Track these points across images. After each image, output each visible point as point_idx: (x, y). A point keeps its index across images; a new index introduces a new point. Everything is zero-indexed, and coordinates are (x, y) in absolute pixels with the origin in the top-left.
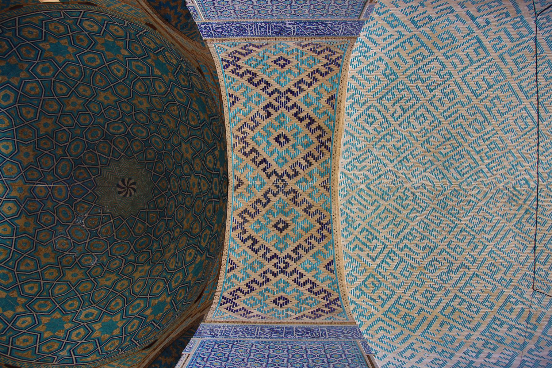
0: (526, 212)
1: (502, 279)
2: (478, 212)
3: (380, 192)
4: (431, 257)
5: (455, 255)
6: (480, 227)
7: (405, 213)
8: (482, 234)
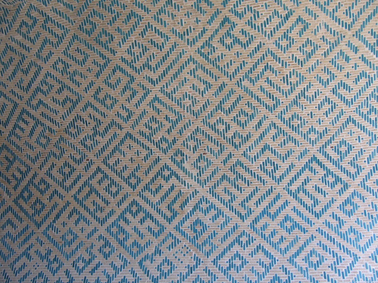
0: (223, 24)
1: (164, 139)
2: (142, 34)
4: (74, 114)
5: (102, 108)
6: (143, 60)
7: (35, 49)
8: (146, 72)
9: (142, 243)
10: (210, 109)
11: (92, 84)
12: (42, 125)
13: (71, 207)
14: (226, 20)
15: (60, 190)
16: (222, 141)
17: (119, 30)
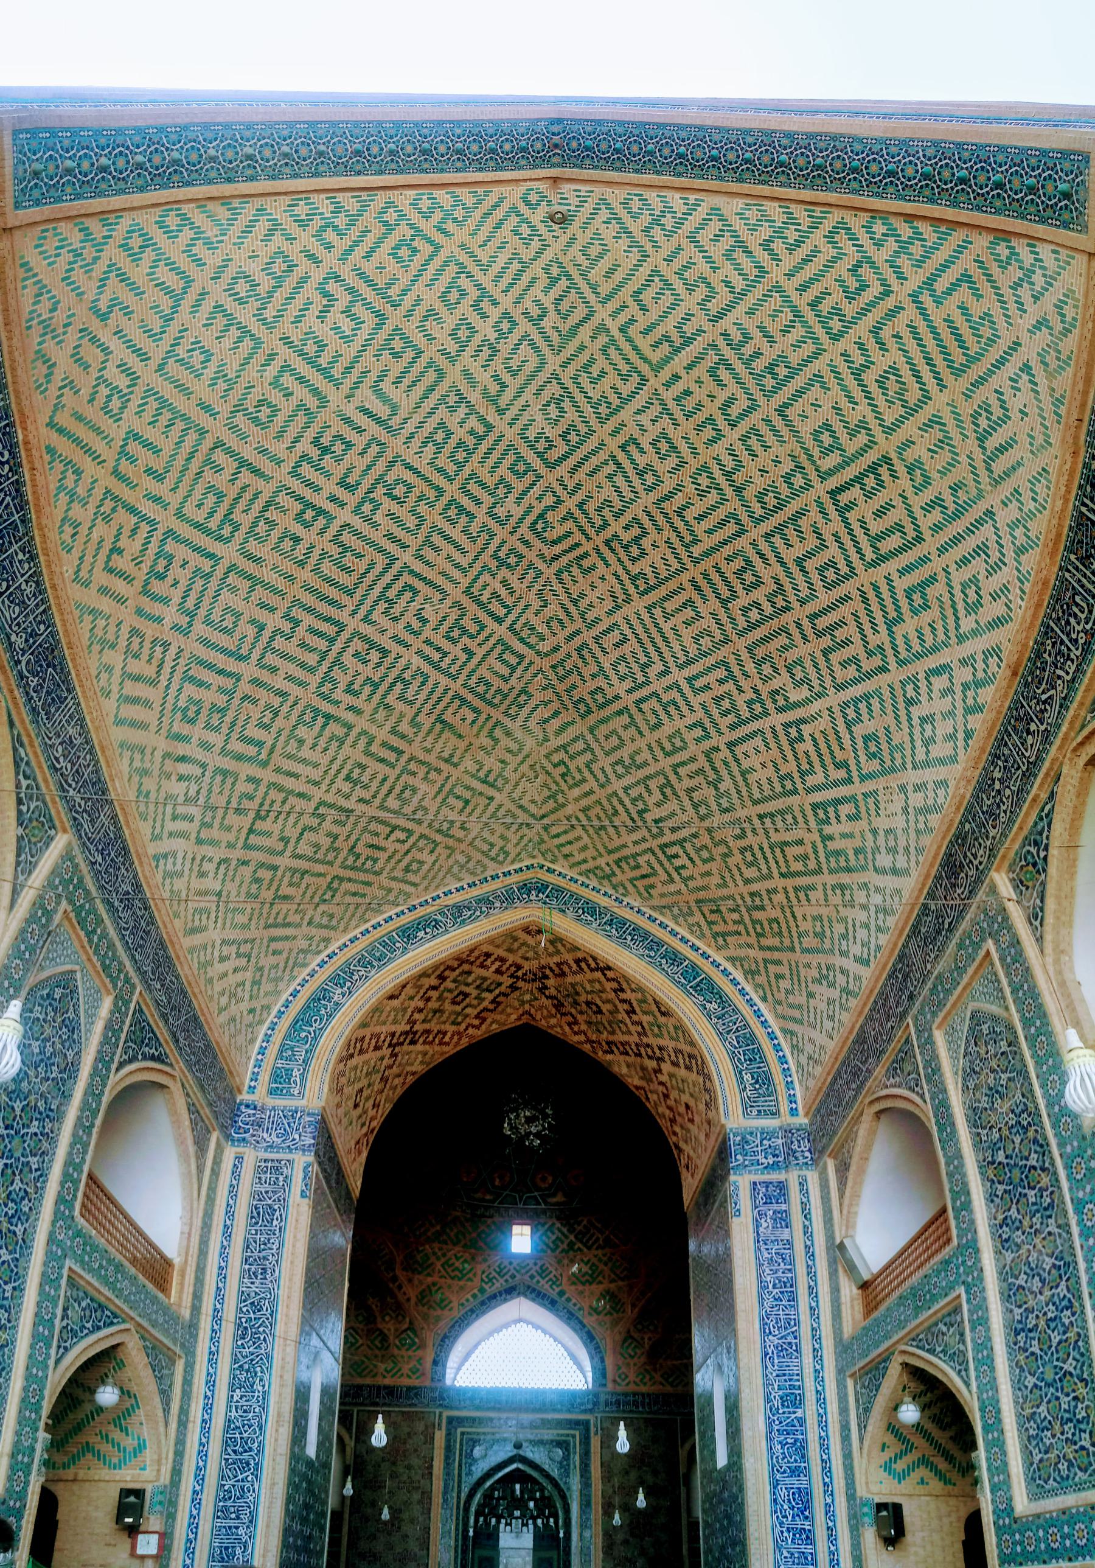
1: (750, 703)
3: (551, 804)
6: (636, 668)
8: (653, 672)
9: (858, 843)
10: (724, 618)
11: (650, 748)
12: (684, 840)
13: (790, 890)
14: (607, 543)
15: (769, 884)
16: (775, 624)
17: (594, 676)
